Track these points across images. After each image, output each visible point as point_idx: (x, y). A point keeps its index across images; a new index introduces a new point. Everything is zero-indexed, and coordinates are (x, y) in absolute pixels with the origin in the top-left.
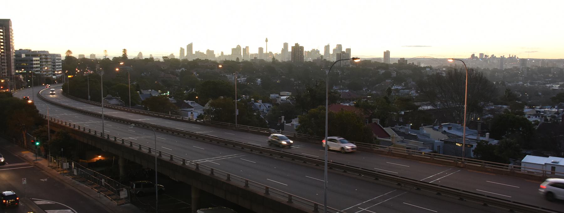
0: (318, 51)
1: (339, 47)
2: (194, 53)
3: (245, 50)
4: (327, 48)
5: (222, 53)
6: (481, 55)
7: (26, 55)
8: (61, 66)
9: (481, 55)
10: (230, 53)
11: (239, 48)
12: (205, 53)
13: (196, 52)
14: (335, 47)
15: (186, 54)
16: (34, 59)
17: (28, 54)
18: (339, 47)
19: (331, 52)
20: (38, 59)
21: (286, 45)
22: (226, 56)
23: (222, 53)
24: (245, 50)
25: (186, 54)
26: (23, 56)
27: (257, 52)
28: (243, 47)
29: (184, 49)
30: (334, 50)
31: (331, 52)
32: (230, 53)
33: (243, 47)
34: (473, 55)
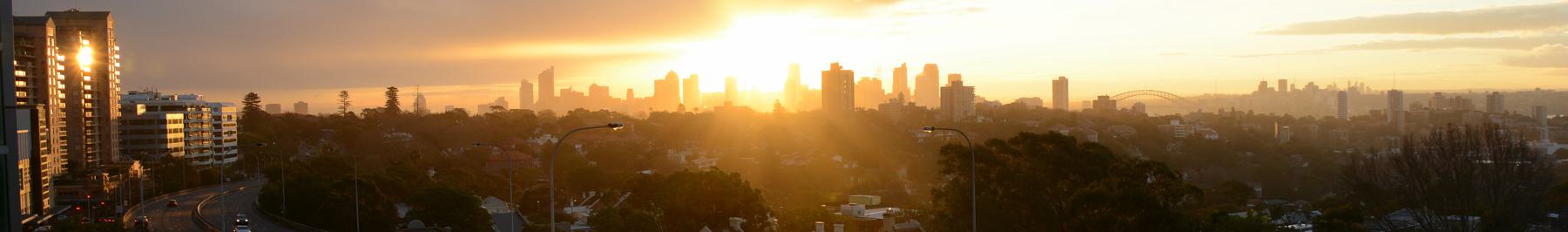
0: (877, 83)
1: (932, 70)
2: (557, 93)
3: (691, 83)
4: (900, 73)
5: (630, 92)
6: (1283, 83)
7: (148, 108)
8: (235, 136)
9: (1283, 83)
11: (672, 76)
12: (587, 94)
13: (562, 91)
14: (920, 71)
15: (536, 97)
16: (169, 116)
17: (153, 103)
18: (932, 70)
19: (911, 85)
20: (180, 116)
22: (640, 100)
23: (630, 92)
24: (691, 83)
25: (536, 97)
26: (141, 110)
29: (531, 86)
30: (919, 80)
31: (911, 85)
34: (1263, 84)
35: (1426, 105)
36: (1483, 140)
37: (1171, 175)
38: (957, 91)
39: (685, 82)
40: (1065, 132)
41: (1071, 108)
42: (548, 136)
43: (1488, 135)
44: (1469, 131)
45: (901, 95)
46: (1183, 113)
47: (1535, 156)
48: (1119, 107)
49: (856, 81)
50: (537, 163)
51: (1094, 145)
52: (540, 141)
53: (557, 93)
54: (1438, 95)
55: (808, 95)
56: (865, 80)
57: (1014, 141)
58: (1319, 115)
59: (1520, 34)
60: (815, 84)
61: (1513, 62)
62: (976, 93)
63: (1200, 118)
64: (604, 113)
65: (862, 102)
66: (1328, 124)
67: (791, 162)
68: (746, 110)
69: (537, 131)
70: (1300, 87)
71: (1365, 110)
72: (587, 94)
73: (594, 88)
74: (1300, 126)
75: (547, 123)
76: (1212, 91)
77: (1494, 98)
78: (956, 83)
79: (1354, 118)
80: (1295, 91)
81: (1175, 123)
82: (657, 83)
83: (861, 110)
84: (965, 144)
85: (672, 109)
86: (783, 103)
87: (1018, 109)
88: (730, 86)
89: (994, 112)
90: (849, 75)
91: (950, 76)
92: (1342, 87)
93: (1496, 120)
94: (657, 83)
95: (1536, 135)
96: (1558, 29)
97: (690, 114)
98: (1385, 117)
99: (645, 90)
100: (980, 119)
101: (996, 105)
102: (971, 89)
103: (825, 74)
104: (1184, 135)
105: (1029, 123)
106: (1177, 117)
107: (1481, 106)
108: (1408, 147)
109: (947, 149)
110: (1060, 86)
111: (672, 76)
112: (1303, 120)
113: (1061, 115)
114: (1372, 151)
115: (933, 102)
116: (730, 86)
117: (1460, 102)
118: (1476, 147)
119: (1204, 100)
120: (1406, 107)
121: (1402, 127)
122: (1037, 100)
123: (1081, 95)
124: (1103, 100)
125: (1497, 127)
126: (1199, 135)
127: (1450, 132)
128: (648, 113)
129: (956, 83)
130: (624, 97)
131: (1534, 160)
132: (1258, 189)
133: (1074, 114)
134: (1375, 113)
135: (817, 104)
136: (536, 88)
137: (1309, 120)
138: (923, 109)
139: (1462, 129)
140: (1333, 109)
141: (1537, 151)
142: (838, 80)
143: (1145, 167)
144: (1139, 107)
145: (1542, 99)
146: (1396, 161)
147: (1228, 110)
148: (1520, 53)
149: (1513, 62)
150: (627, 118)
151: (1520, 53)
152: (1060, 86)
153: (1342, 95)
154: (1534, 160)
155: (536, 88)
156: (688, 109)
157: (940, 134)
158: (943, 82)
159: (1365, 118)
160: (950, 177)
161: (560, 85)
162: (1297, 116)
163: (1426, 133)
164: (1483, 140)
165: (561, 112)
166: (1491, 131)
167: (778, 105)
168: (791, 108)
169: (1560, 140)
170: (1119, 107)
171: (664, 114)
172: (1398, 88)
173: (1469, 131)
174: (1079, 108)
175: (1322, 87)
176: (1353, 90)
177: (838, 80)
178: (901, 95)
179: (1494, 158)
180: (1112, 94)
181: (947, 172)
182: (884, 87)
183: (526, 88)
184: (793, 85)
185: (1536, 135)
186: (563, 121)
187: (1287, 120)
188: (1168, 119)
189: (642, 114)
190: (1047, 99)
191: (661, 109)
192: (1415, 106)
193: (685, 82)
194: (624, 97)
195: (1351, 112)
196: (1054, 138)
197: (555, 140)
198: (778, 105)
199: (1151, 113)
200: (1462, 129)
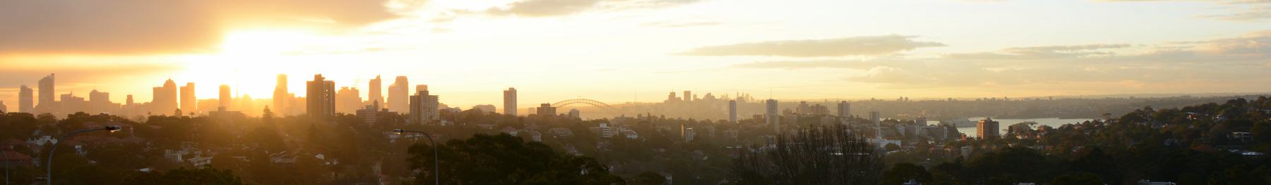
0: (355, 92)
1: (402, 82)
2: (57, 98)
3: (188, 90)
4: (375, 84)
5: (130, 98)
6: (687, 94)
9: (687, 94)
10: (150, 99)
11: (170, 85)
12: (87, 99)
13: (63, 96)
14: (392, 82)
15: (36, 102)
18: (402, 82)
19: (385, 94)
21: (283, 80)
22: (139, 106)
23: (130, 98)
24: (188, 90)
25: (36, 102)
27: (216, 96)
28: (180, 83)
29: (31, 91)
30: (391, 89)
31: (385, 94)
32: (150, 99)
33: (180, 83)
34: (673, 95)
35: (794, 111)
36: (836, 138)
37: (600, 169)
38: (423, 99)
39: (182, 89)
40: (514, 133)
41: (519, 113)
42: (48, 138)
43: (839, 135)
44: (825, 130)
45: (376, 102)
46: (610, 117)
47: (872, 149)
48: (558, 112)
49: (337, 89)
50: (36, 162)
51: (538, 144)
52: (40, 142)
53: (57, 98)
54: (803, 103)
55: (293, 100)
56: (345, 89)
57: (471, 142)
58: (715, 119)
59: (863, 58)
60: (299, 90)
61: (867, 80)
62: (440, 101)
63: (624, 122)
64: (104, 117)
65: (341, 108)
66: (722, 126)
67: (278, 160)
68: (238, 116)
69: (37, 133)
70: (701, 96)
71: (749, 115)
72: (87, 99)
73: (94, 94)
74: (701, 128)
75: (46, 124)
76: (632, 100)
77: (843, 106)
78: (423, 93)
79: (741, 121)
80: (696, 100)
81: (604, 126)
82: (156, 90)
83: (341, 115)
84: (429, 144)
85: (169, 113)
86: (272, 109)
87: (476, 115)
88: (224, 91)
89: (452, 115)
90: (331, 85)
91: (418, 87)
92: (733, 97)
93: (844, 122)
94: (156, 90)
95: (872, 134)
96: (888, 55)
97: (186, 118)
98: (765, 121)
99: (144, 96)
100: (443, 123)
101: (457, 110)
102: (435, 98)
103: (309, 84)
104: (610, 135)
105: (485, 126)
106: (605, 121)
107: (834, 112)
108: (781, 142)
109: (413, 149)
110: (510, 95)
111: (170, 85)
112: (703, 123)
113: (510, 119)
114: (755, 147)
115: (403, 109)
116: (224, 91)
117: (819, 108)
118: (831, 142)
119: (627, 106)
120: (780, 113)
121: (777, 128)
122: (491, 107)
123: (527, 103)
124: (546, 109)
125: (845, 127)
126: (622, 135)
127: (812, 131)
128: (146, 117)
129: (423, 93)
130: (124, 102)
131: (871, 152)
132: (669, 178)
133: (521, 119)
134: (757, 117)
135: (303, 110)
136: (36, 93)
137: (709, 122)
138: (394, 115)
139: (820, 129)
140: (726, 116)
141: (873, 146)
142: (321, 90)
143: (579, 161)
144: (574, 113)
145: (876, 107)
146: (773, 154)
147: (645, 115)
148: (862, 73)
149: (855, 79)
150: (126, 121)
151: (862, 73)
152: (510, 95)
153: (732, 103)
154: (871, 152)
155: (36, 93)
156: (184, 114)
157: (409, 136)
158: (412, 91)
159: (750, 121)
160: (417, 171)
161: (59, 92)
162: (698, 120)
163: (795, 132)
164: (836, 138)
165: (61, 115)
166: (840, 130)
167: (267, 110)
168: (279, 113)
169: (889, 137)
170: (558, 112)
171: (162, 118)
172: (774, 98)
173: (825, 130)
174: (526, 114)
175: (718, 97)
176: (740, 99)
177: (321, 90)
178: (376, 102)
179: (843, 151)
180: (552, 102)
181: (413, 168)
182: (361, 95)
183: (25, 93)
184: (281, 92)
185: (872, 134)
186: (63, 123)
187: (691, 122)
188: (597, 122)
189: (141, 118)
190: (500, 107)
191: (159, 114)
192: (787, 111)
193: (182, 89)
194: (124, 102)
195: (740, 116)
196: (505, 138)
197: (54, 141)
198: (267, 110)
199: (584, 118)
200: (820, 129)
